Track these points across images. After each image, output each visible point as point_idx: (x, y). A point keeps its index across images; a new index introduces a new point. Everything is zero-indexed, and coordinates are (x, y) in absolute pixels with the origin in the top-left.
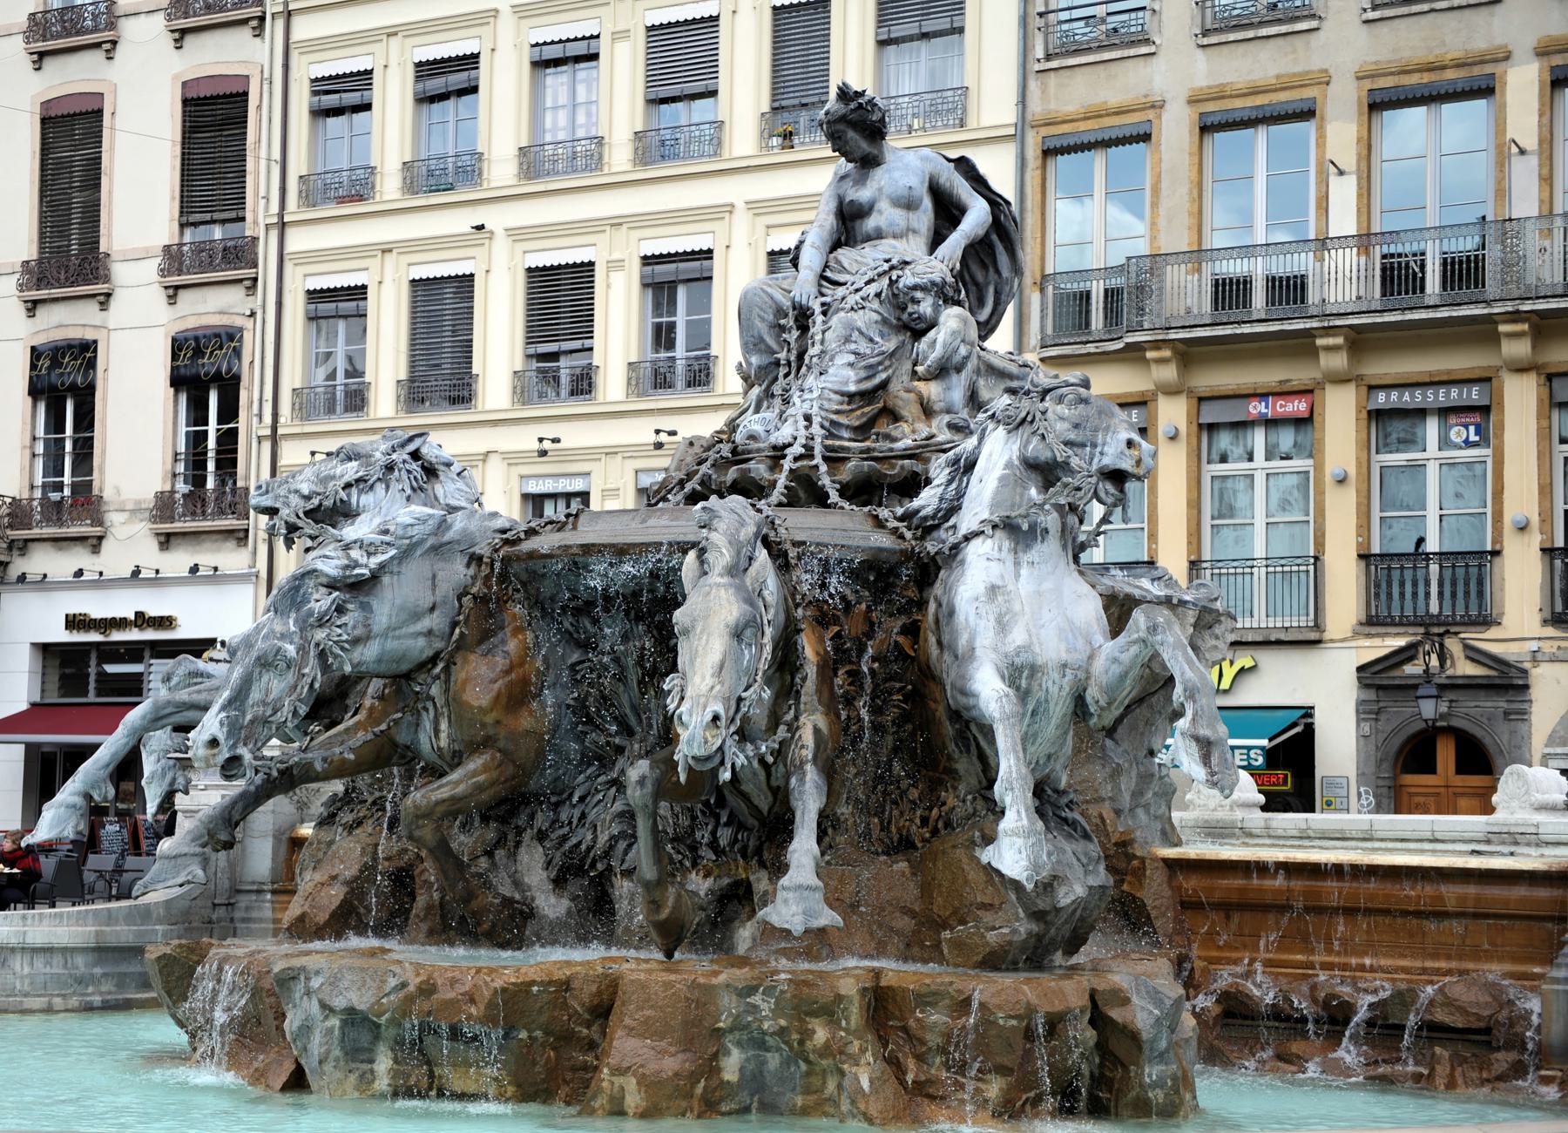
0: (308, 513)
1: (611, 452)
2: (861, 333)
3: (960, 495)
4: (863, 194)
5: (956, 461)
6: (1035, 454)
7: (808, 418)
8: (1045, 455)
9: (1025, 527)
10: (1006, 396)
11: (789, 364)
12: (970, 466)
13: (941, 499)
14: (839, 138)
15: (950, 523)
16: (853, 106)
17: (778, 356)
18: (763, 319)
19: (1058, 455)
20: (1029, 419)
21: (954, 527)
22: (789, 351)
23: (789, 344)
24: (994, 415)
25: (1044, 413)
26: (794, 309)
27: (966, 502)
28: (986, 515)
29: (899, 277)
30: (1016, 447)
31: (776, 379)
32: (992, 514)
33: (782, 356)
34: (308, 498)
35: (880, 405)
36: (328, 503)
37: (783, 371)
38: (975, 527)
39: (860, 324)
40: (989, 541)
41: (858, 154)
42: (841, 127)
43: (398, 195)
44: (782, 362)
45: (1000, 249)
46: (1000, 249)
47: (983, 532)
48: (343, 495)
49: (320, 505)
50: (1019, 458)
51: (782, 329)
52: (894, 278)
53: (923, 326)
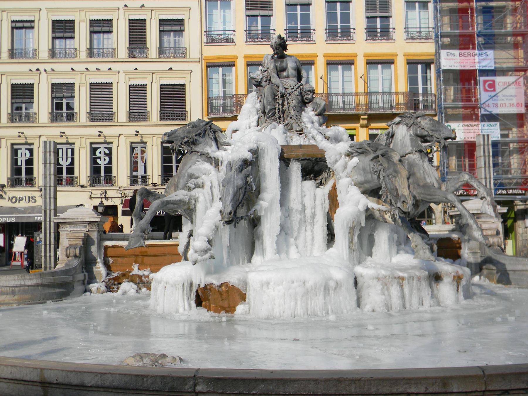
0: (185, 143)
1: (81, 137)
4: (284, 65)
5: (388, 134)
8: (426, 133)
9: (425, 152)
11: (279, 109)
12: (393, 136)
20: (415, 123)
22: (279, 105)
25: (420, 122)
26: (280, 94)
30: (411, 132)
32: (413, 148)
33: (277, 106)
34: (183, 138)
36: (191, 140)
37: (277, 111)
38: (408, 152)
43: (6, 58)
48: (195, 138)
49: (188, 141)
50: (413, 134)
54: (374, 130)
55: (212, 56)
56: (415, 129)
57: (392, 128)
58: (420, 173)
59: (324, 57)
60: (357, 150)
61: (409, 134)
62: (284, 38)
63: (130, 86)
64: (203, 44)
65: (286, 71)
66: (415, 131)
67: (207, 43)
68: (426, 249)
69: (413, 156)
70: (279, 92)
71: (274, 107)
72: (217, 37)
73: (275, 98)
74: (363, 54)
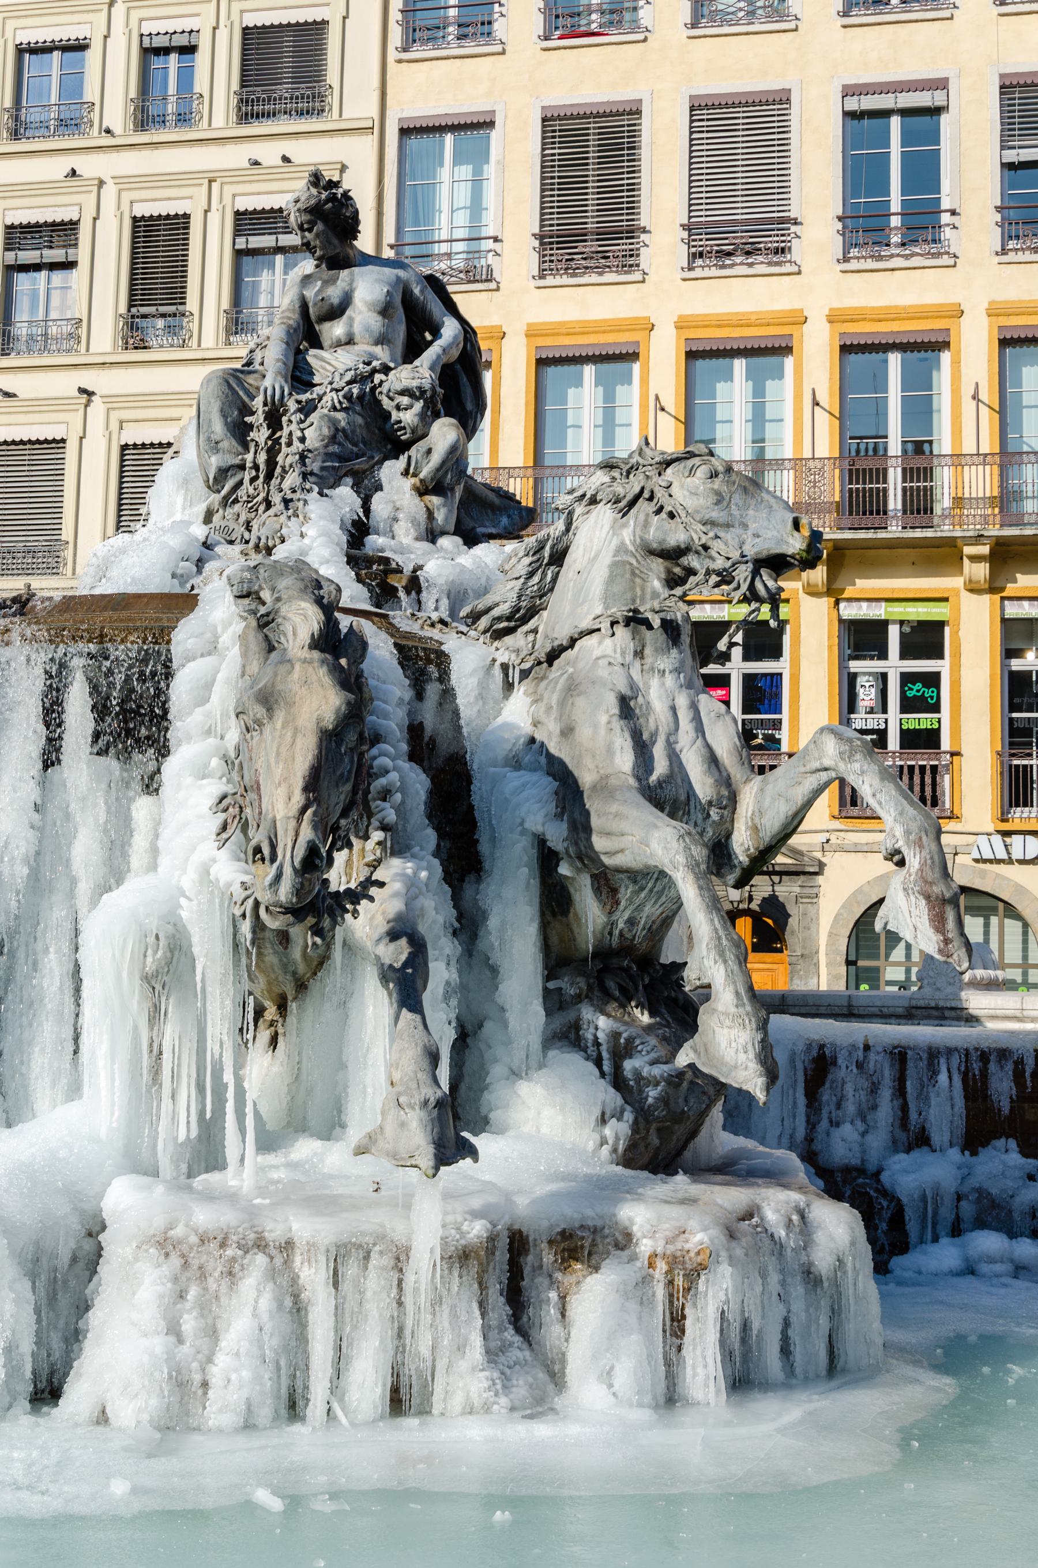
3: (545, 591)
6: (659, 536)
8: (677, 537)
10: (599, 473)
11: (256, 467)
12: (558, 558)
13: (519, 597)
15: (532, 623)
19: (695, 537)
20: (646, 495)
21: (535, 631)
23: (257, 445)
24: (584, 496)
26: (265, 404)
27: (553, 599)
28: (599, 610)
31: (240, 483)
32: (607, 608)
38: (586, 624)
40: (608, 642)
44: (248, 465)
45: (464, 379)
46: (464, 379)
47: (599, 630)
50: (633, 543)
51: (250, 427)
52: (376, 381)
54: (1026, 604)
56: (642, 517)
57: (569, 525)
58: (595, 727)
59: (830, 322)
61: (615, 542)
63: (124, 447)
65: (345, 317)
66: (638, 530)
68: (412, 1107)
69: (600, 643)
74: (986, 306)
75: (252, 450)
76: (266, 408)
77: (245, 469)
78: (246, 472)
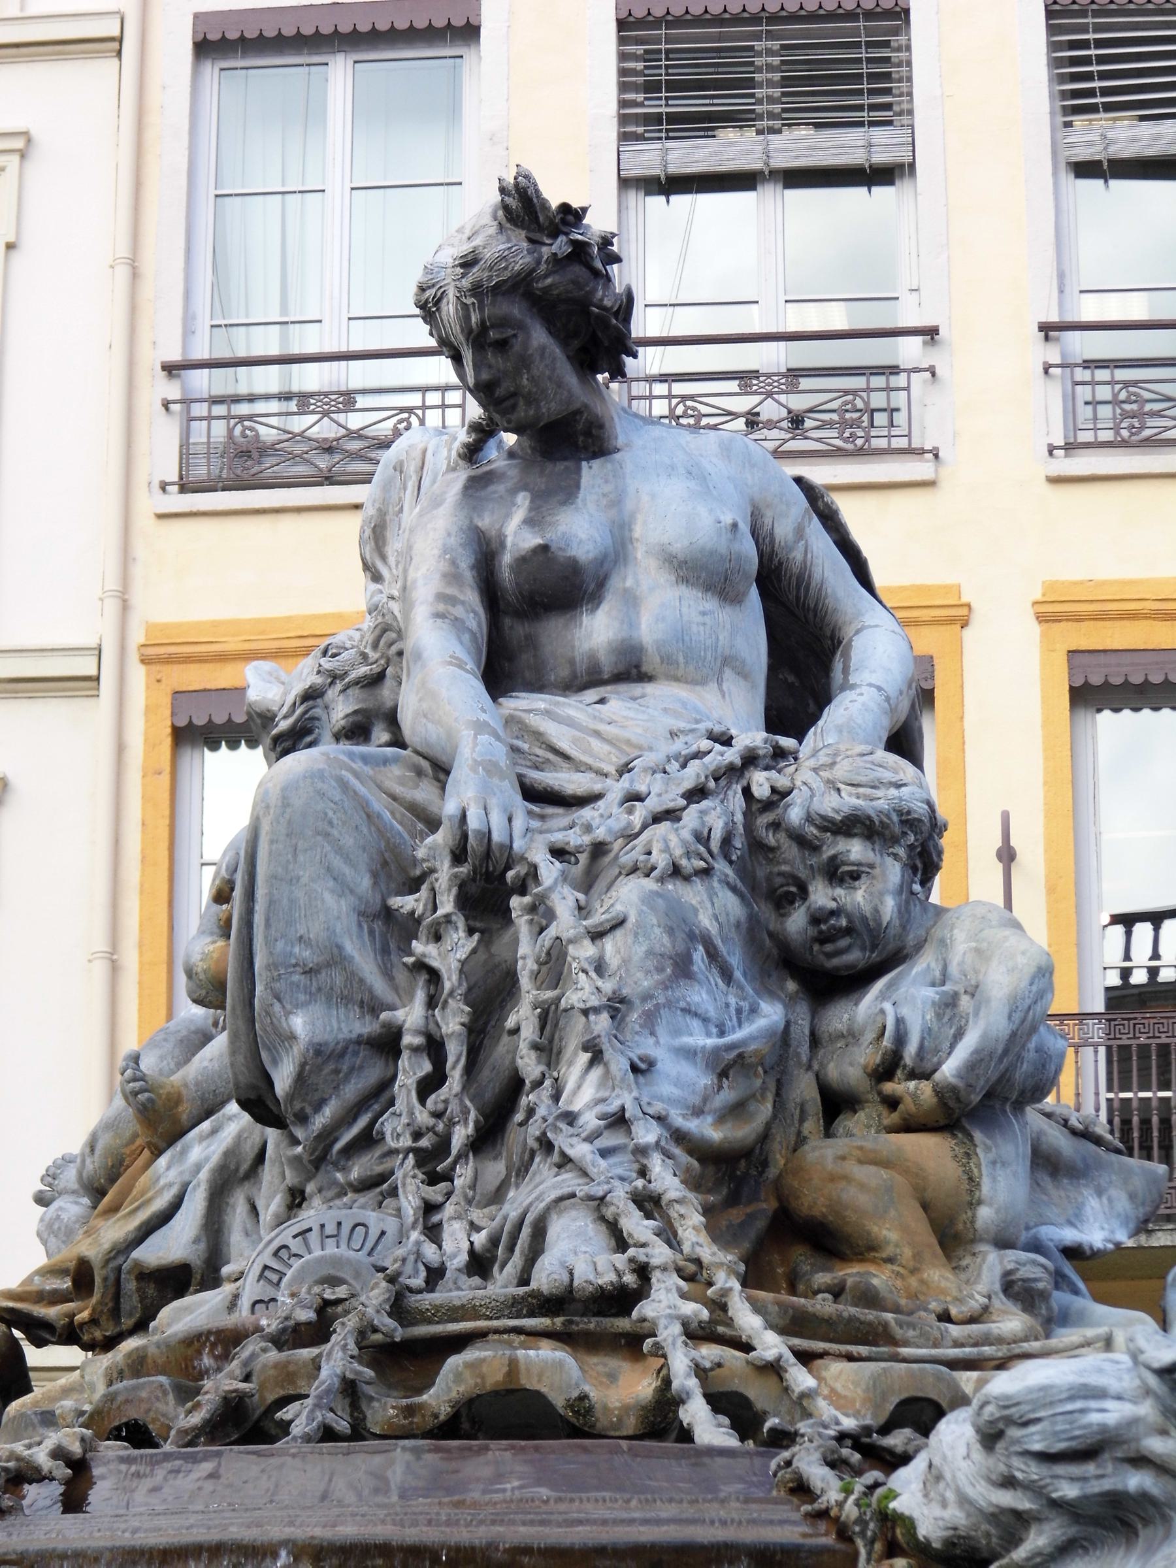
2: (712, 954)
7: (649, 1203)
11: (434, 1047)
14: (502, 345)
16: (560, 246)
17: (400, 1014)
18: (343, 887)
22: (432, 1003)
23: (434, 976)
26: (459, 856)
29: (780, 795)
35: (768, 1205)
39: (706, 921)
41: (551, 408)
42: (515, 309)
44: (408, 1039)
51: (408, 927)
53: (855, 957)
55: (234, 625)
60: (1033, 1471)
62: (571, 216)
64: (149, 502)
67: (184, 488)
70: (441, 838)
71: (366, 1027)
72: (299, 423)
73: (388, 914)
75: (420, 996)
76: (464, 870)
77: (397, 1053)
78: (404, 1062)
